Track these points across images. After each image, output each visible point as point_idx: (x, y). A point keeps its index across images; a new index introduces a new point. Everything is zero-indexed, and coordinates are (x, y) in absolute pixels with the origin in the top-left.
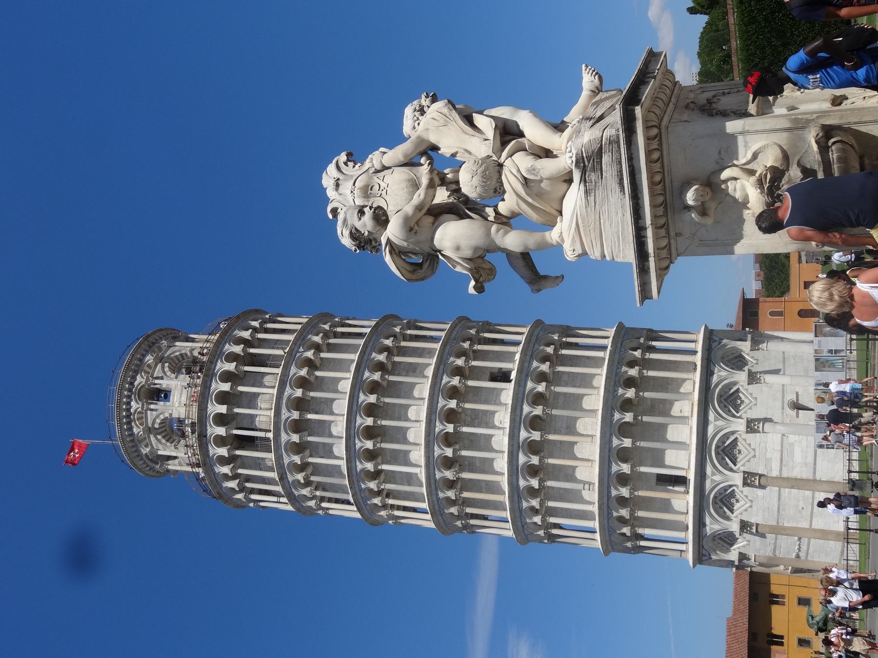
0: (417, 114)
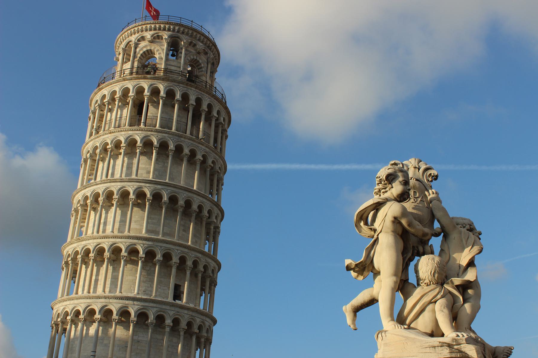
0: (468, 227)
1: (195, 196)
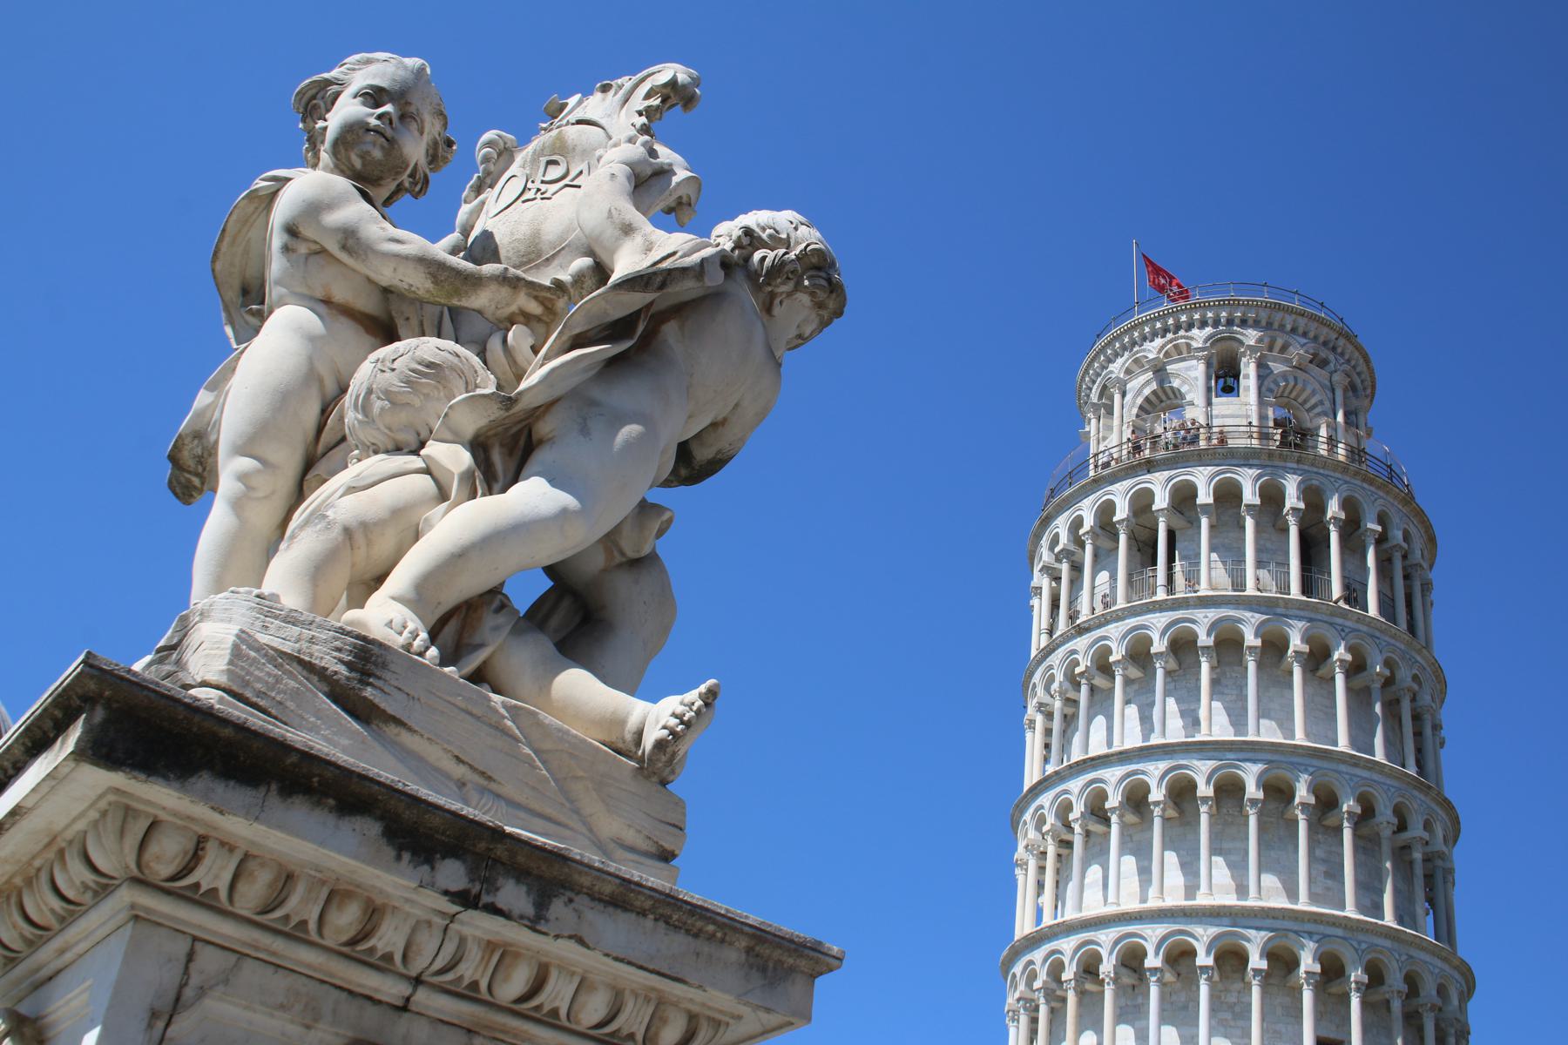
1: (1343, 768)
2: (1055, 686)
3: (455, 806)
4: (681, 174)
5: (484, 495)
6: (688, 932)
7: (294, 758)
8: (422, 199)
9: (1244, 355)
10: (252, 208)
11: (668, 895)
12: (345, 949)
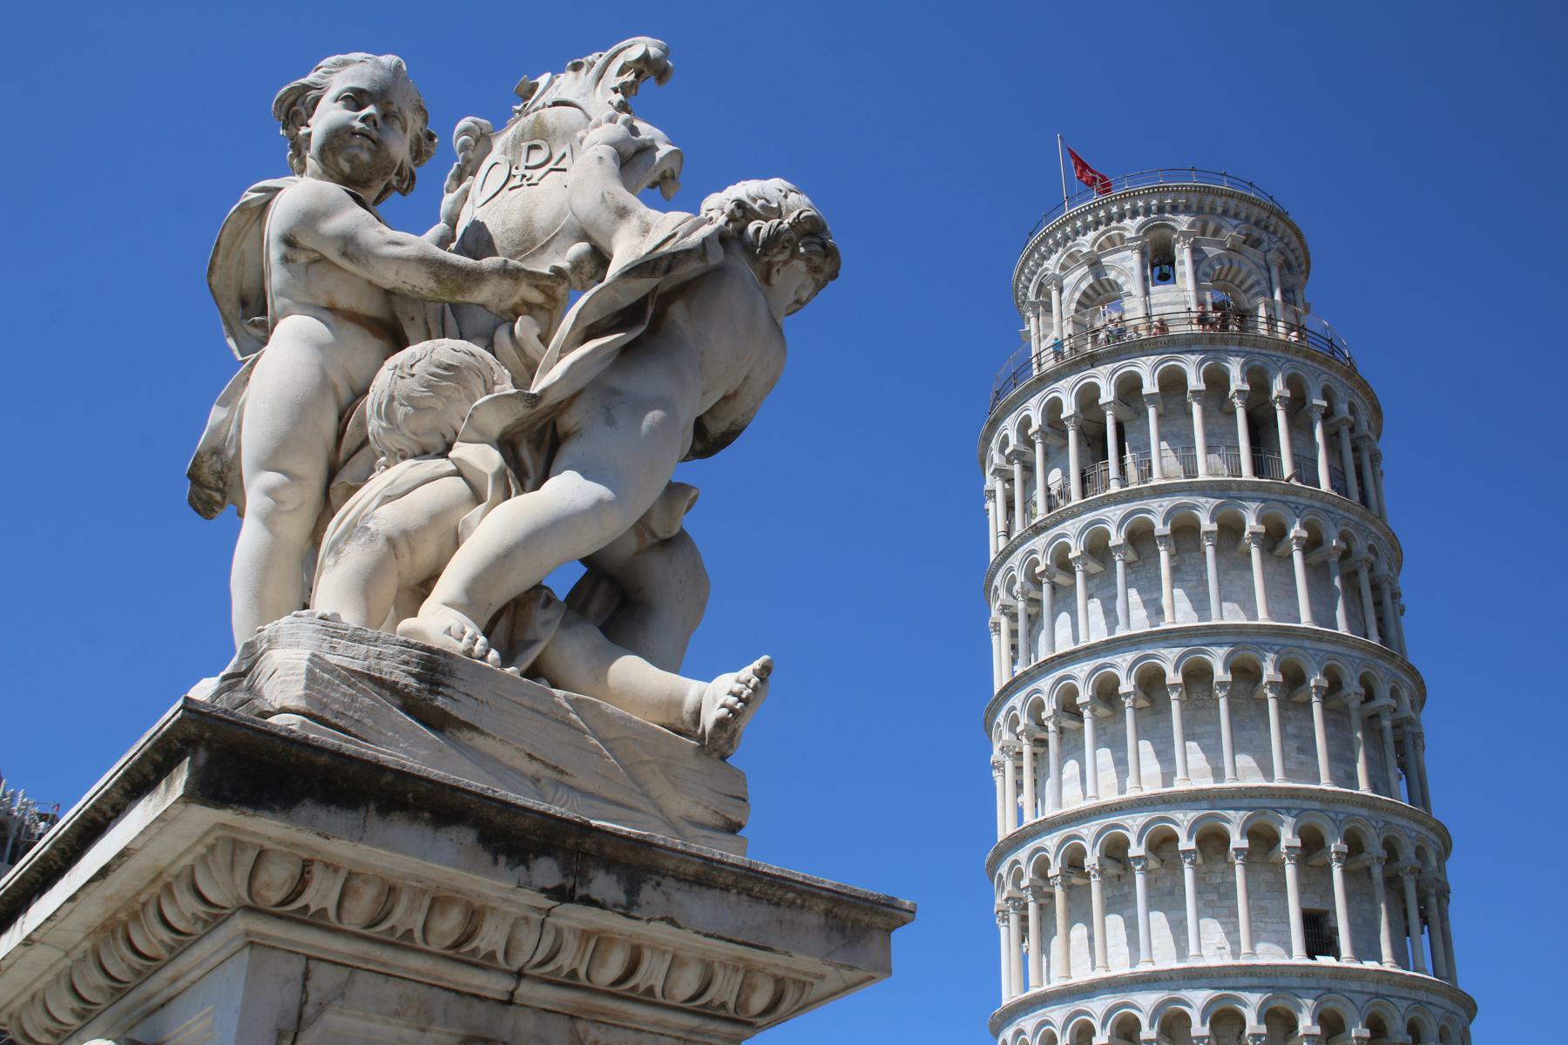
1: (1307, 644)
2: (1017, 587)
3: (543, 807)
4: (664, 149)
5: (518, 493)
6: (769, 902)
7: (389, 778)
8: (410, 195)
9: (1177, 241)
10: (243, 220)
11: (749, 869)
12: (449, 953)
